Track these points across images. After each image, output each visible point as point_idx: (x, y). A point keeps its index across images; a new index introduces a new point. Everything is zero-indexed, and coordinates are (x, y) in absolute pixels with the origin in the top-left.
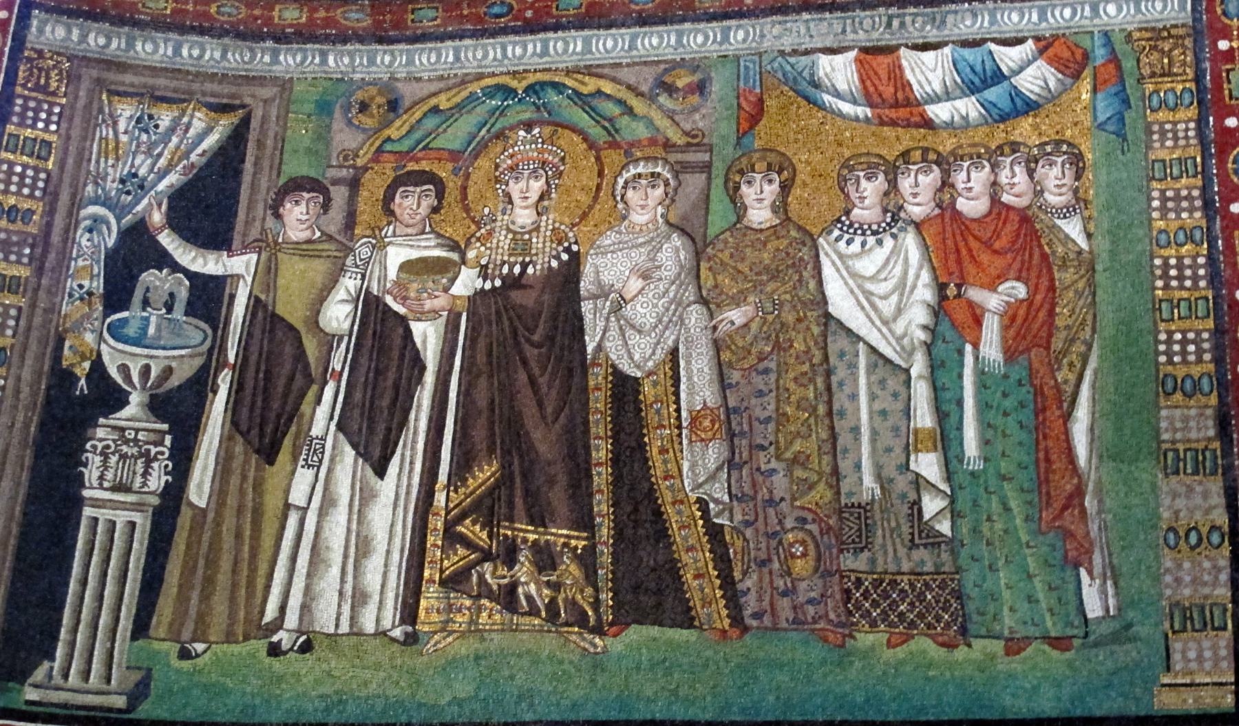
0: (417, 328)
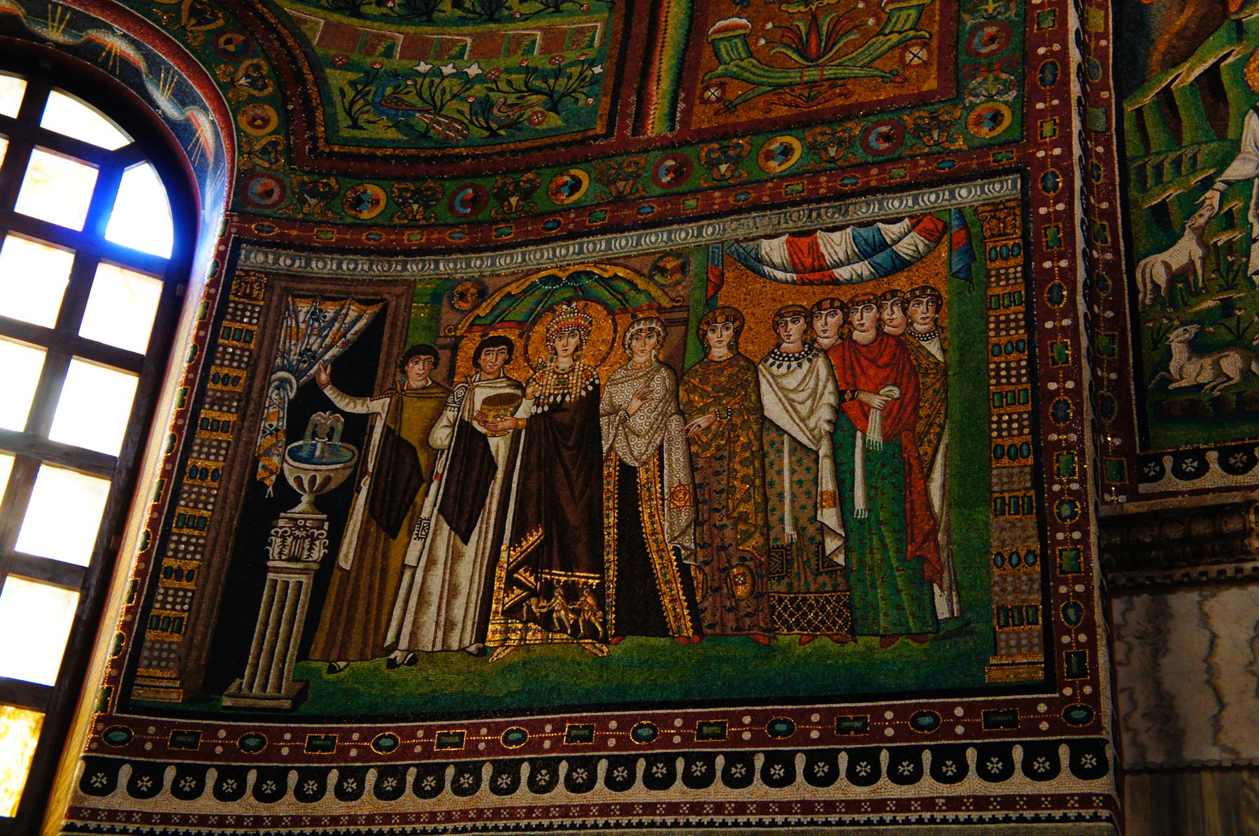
0: (493, 442)
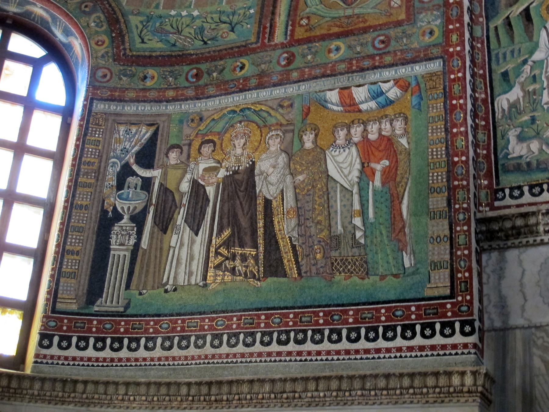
0: (208, 189)
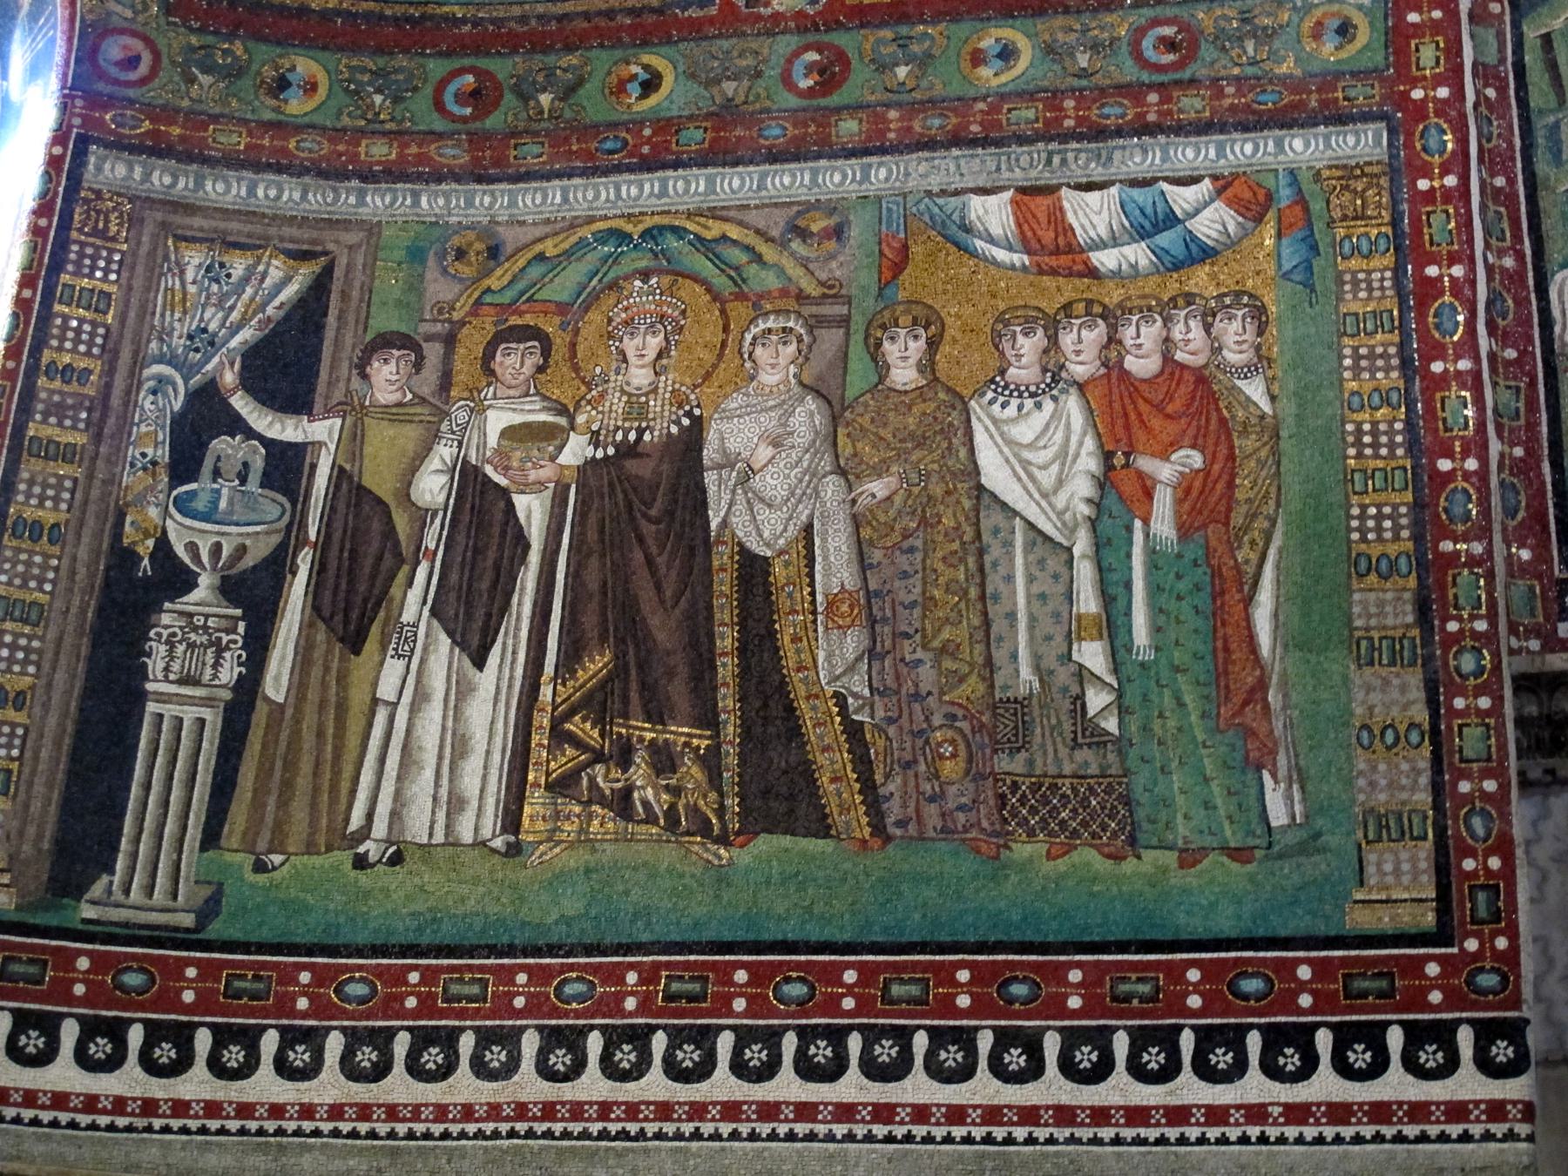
0: (521, 502)
